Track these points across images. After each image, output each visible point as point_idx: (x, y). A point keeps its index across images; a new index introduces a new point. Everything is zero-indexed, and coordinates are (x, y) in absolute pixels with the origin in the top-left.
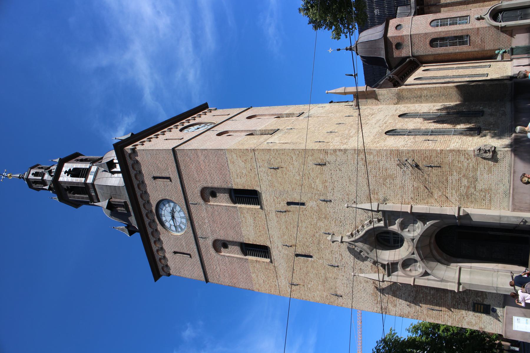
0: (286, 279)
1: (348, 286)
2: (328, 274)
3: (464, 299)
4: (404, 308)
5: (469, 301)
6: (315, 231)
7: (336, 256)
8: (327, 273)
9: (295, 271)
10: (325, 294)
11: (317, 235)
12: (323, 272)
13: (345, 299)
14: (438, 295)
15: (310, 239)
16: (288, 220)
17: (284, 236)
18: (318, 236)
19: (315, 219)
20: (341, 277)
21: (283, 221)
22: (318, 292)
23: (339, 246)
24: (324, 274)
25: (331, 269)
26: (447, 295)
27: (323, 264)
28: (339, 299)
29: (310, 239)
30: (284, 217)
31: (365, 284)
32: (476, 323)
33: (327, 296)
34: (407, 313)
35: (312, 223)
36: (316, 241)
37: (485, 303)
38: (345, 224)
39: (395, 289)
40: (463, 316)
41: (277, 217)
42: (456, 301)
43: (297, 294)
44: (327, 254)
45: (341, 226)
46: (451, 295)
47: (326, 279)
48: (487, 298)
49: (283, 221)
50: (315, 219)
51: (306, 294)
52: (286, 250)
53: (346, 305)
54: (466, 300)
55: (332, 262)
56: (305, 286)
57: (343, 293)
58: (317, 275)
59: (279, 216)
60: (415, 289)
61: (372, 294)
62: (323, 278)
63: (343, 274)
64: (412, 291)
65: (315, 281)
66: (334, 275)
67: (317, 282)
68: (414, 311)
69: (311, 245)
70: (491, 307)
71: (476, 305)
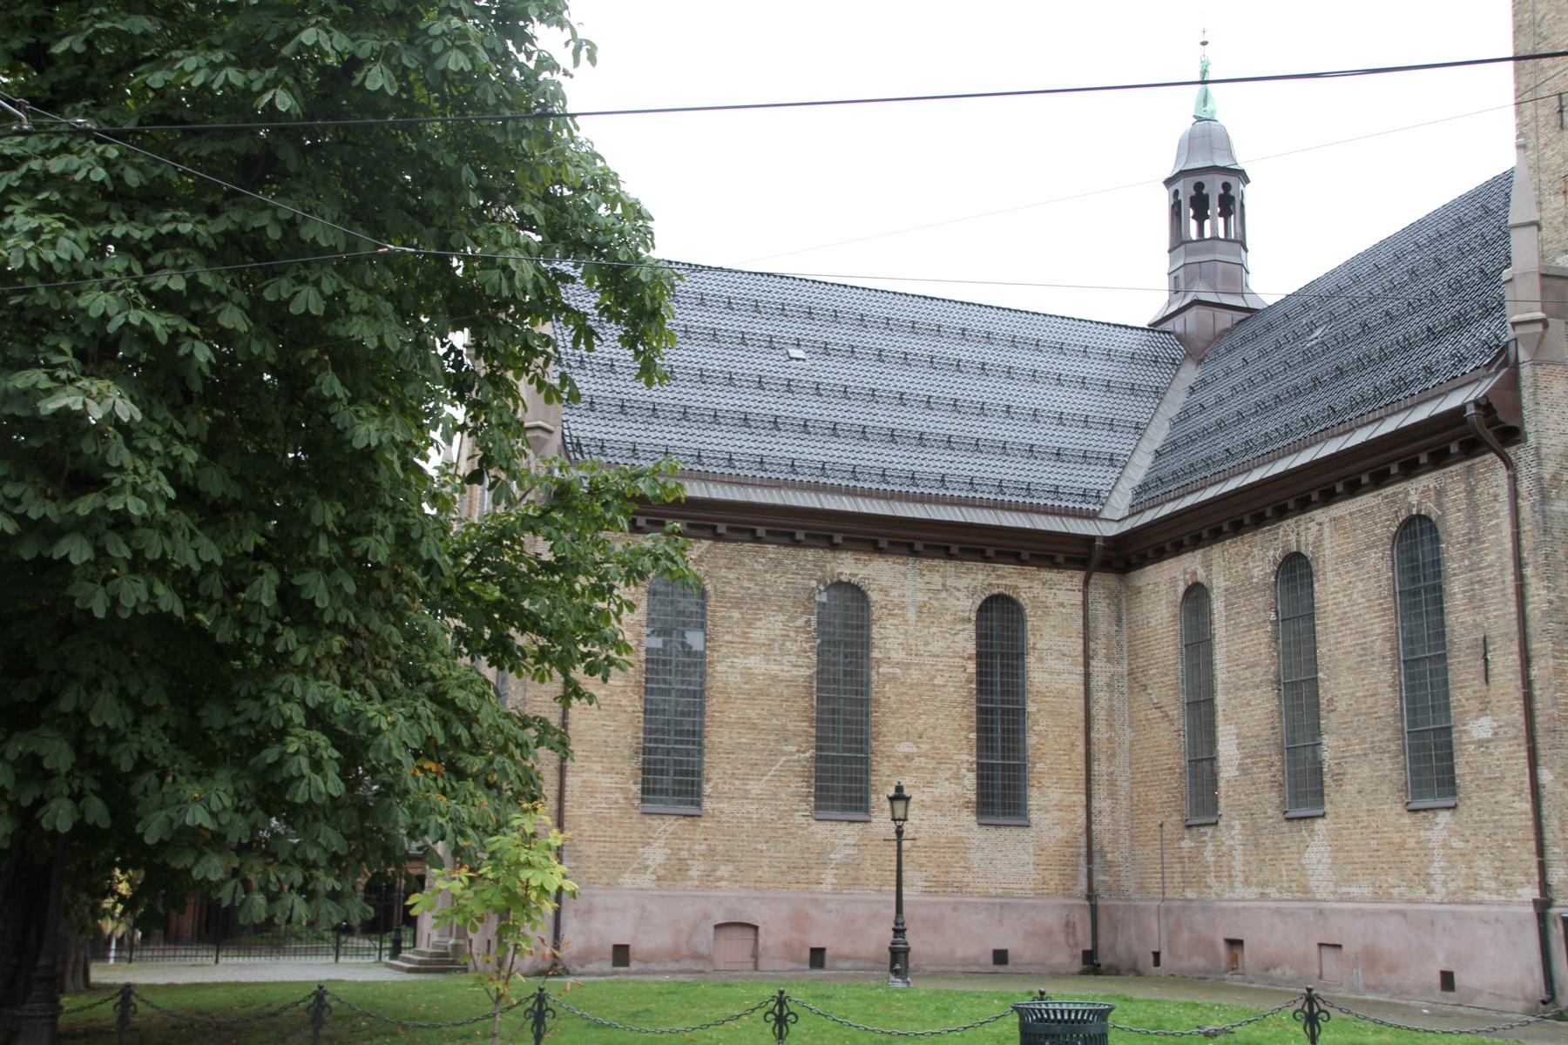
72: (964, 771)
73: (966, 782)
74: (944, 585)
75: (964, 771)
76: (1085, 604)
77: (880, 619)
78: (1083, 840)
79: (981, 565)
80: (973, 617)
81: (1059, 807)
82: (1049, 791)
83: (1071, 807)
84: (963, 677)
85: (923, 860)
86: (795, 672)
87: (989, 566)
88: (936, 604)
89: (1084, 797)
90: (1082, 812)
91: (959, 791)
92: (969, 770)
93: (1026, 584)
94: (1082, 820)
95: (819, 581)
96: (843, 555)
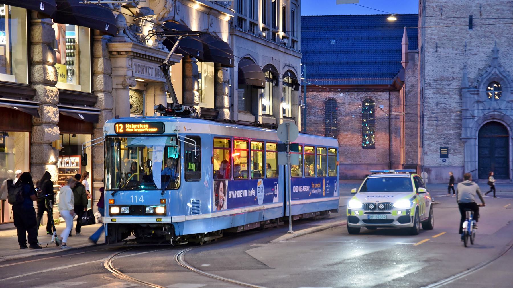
0: (445, 3)
1: (447, 58)
2: (456, 42)
3: (450, 141)
4: (434, 100)
5: (449, 145)
6: (496, 35)
7: (474, 50)
8: (457, 41)
9: (455, 13)
10: (436, 37)
11: (493, 36)
12: (458, 37)
13: (433, 53)
14: (451, 125)
15: (488, 30)
16: (506, 12)
17: (489, 6)
18: (492, 36)
19: (507, 35)
20: (455, 52)
21: (504, 8)
22: (436, 31)
23: (484, 53)
24: (456, 38)
25: (462, 45)
26: (452, 130)
27: (466, 38)
28: (433, 49)
29: (488, 30)
30: (508, 9)
31: (451, 71)
32: (430, 150)
33: (434, 39)
34: (430, 102)
35: (503, 33)
36: (487, 34)
37: (449, 155)
38: (505, 59)
39: (450, 94)
40: (435, 141)
41: (507, 3)
42: (447, 137)
43: (430, 11)
44: (475, 43)
45: (503, 56)
46: (452, 133)
47: (451, 40)
48: (454, 156)
49: (504, 8)
50: (507, 35)
51: (432, 21)
52: (475, 7)
53: (428, 55)
54: (449, 143)
55: (468, 46)
56: (441, 21)
57: (440, 53)
58: (454, 32)
59: (509, 4)
60: (453, 108)
61: (442, 77)
62: (452, 37)
63: (458, 55)
64: (450, 107)
65: (447, 30)
66: (456, 47)
67: (447, 32)
68: (432, 108)
69: (483, 30)
70: (446, 159)
71: (446, 149)
72: (359, 138)
73: (360, 140)
74: (354, 98)
75: (359, 138)
76: (389, 99)
77: (339, 106)
78: (388, 151)
79: (363, 92)
80: (362, 104)
81: (383, 144)
82: (380, 141)
83: (385, 144)
84: (359, 117)
85: (350, 157)
86: (320, 119)
87: (365, 93)
88: (352, 102)
89: (388, 142)
90: (388, 145)
91: (358, 142)
92: (360, 137)
93: (375, 96)
94: (388, 147)
95: (325, 99)
96: (331, 93)
